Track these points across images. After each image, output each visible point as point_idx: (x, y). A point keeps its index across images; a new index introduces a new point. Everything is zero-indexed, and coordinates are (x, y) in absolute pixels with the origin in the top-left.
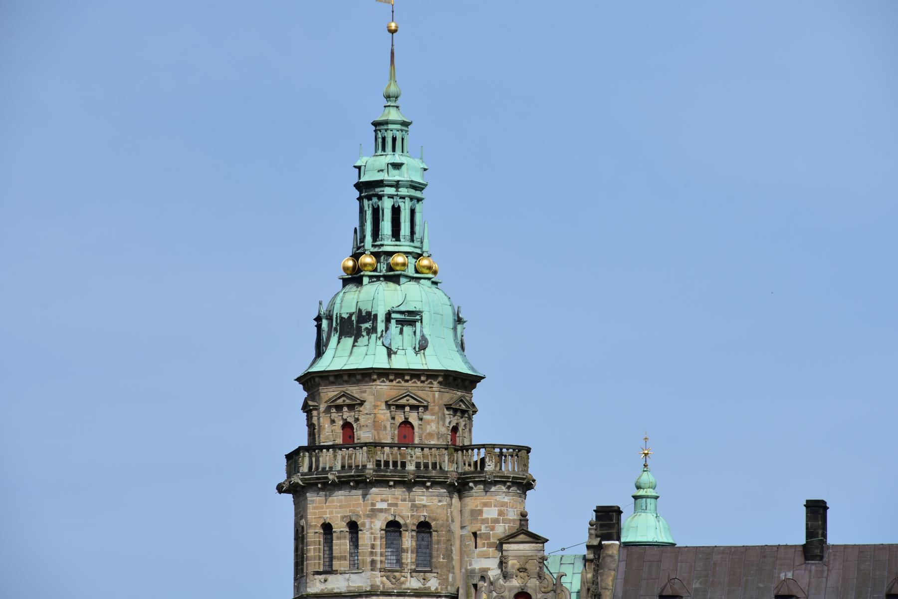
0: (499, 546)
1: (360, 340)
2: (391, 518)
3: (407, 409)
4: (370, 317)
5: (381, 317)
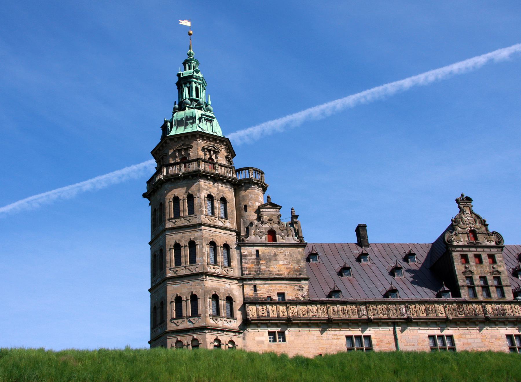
0: (258, 211)
1: (188, 127)
2: (209, 193)
3: (212, 152)
4: (193, 118)
5: (197, 118)
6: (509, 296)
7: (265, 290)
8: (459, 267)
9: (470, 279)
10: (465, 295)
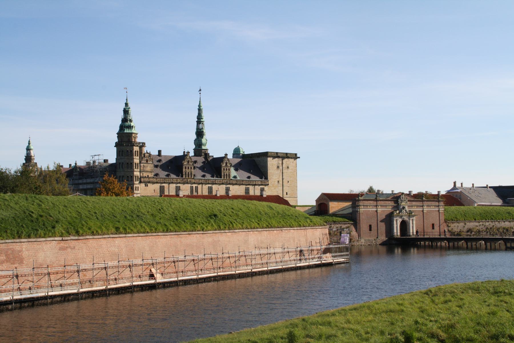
6: (193, 177)
7: (145, 174)
8: (184, 170)
9: (186, 173)
10: (184, 176)
